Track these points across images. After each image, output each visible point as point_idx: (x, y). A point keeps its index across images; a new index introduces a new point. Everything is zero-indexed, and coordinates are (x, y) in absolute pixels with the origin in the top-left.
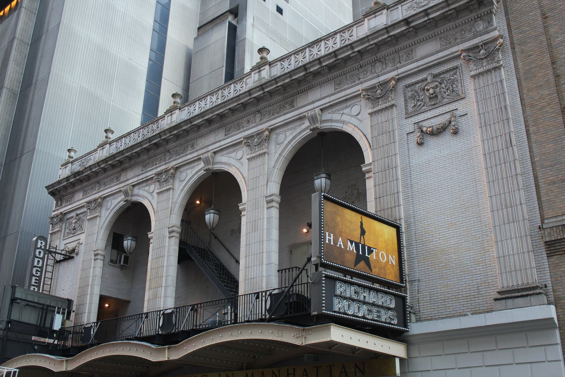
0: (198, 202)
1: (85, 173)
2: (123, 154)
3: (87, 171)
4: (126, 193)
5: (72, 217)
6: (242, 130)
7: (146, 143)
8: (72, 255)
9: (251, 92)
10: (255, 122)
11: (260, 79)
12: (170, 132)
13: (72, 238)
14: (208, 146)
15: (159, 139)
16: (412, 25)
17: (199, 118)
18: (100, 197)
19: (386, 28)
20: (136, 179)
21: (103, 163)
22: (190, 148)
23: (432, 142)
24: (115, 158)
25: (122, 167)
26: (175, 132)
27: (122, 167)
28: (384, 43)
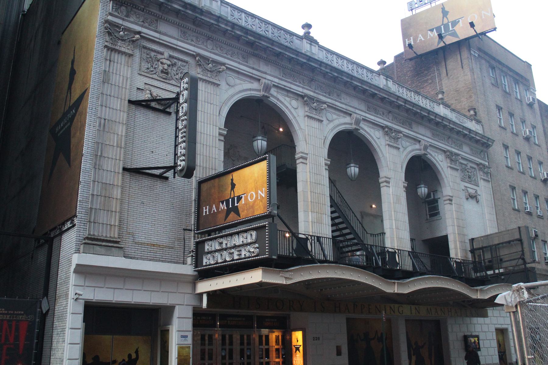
0: (281, 130)
1: (205, 16)
2: (272, 45)
3: (210, 18)
4: (267, 88)
5: (162, 54)
6: (379, 116)
7: (303, 58)
8: (168, 110)
9: (399, 98)
10: (388, 118)
11: (387, 85)
12: (331, 70)
13: (158, 82)
14: (356, 108)
15: (319, 67)
16: (471, 135)
17: (359, 82)
18: (224, 64)
19: (450, 121)
20: (276, 80)
21: (241, 31)
22: (335, 95)
23: (470, 199)
24: (260, 39)
25: (256, 52)
26: (336, 74)
27: (256, 52)
28: (458, 132)
